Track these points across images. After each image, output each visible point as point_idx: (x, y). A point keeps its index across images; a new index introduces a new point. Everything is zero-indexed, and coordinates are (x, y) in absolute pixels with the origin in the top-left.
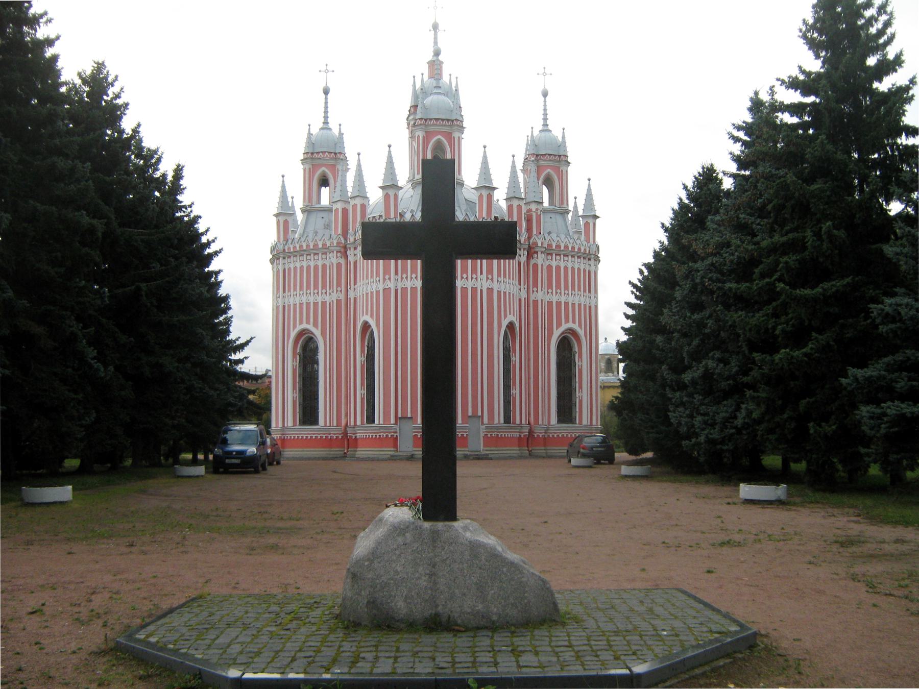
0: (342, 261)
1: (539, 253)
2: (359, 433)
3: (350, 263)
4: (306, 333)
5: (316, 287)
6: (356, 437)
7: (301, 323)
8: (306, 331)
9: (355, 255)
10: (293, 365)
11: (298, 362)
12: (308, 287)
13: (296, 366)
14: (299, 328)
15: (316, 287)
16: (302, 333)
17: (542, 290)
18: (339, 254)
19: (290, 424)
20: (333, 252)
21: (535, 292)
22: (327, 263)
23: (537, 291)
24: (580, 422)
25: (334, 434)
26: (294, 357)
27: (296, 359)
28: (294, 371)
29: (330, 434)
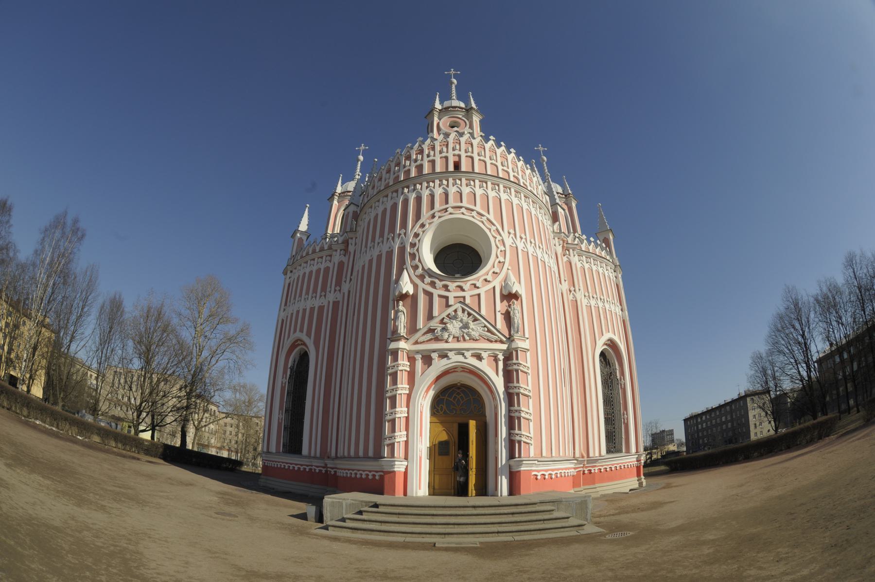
0: (345, 259)
1: (571, 250)
2: (342, 469)
3: (350, 253)
4: (299, 345)
5: (315, 291)
6: (335, 472)
7: (295, 331)
8: (299, 342)
9: (356, 244)
10: (282, 382)
11: (288, 376)
12: (307, 293)
13: (285, 383)
14: (293, 337)
15: (315, 291)
16: (293, 346)
17: (579, 290)
18: (342, 252)
19: (273, 449)
20: (336, 251)
21: (573, 292)
22: (331, 265)
23: (575, 291)
24: (628, 450)
25: (317, 467)
26: (285, 372)
27: (286, 375)
28: (283, 389)
29: (312, 466)
